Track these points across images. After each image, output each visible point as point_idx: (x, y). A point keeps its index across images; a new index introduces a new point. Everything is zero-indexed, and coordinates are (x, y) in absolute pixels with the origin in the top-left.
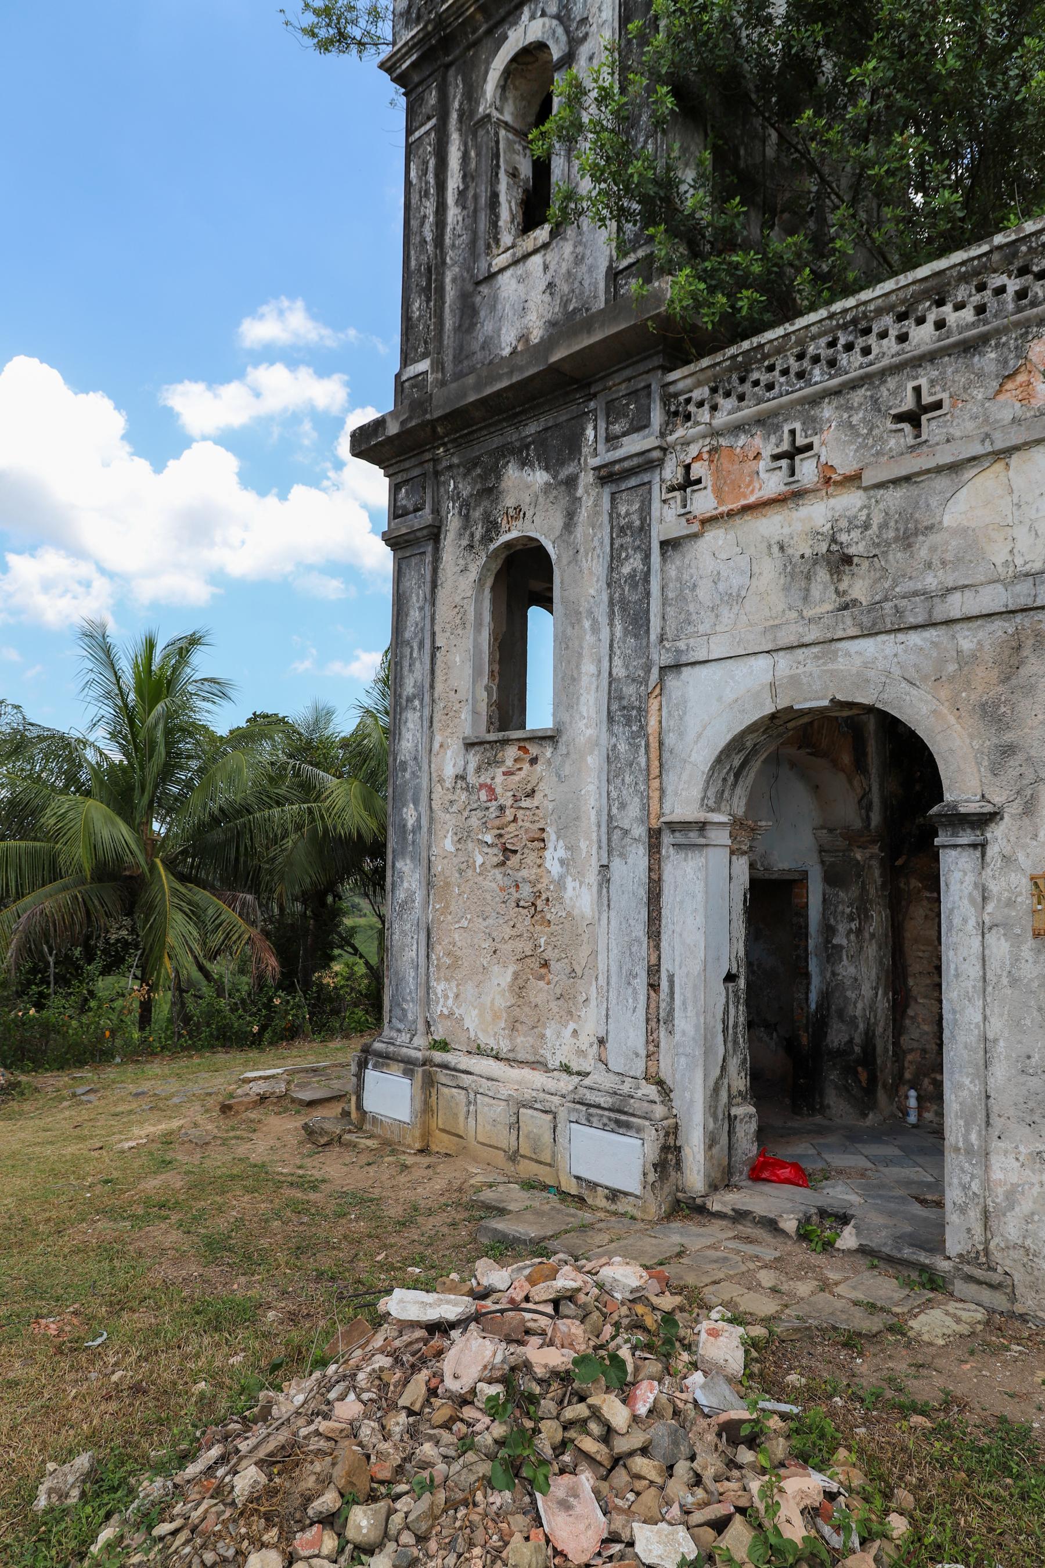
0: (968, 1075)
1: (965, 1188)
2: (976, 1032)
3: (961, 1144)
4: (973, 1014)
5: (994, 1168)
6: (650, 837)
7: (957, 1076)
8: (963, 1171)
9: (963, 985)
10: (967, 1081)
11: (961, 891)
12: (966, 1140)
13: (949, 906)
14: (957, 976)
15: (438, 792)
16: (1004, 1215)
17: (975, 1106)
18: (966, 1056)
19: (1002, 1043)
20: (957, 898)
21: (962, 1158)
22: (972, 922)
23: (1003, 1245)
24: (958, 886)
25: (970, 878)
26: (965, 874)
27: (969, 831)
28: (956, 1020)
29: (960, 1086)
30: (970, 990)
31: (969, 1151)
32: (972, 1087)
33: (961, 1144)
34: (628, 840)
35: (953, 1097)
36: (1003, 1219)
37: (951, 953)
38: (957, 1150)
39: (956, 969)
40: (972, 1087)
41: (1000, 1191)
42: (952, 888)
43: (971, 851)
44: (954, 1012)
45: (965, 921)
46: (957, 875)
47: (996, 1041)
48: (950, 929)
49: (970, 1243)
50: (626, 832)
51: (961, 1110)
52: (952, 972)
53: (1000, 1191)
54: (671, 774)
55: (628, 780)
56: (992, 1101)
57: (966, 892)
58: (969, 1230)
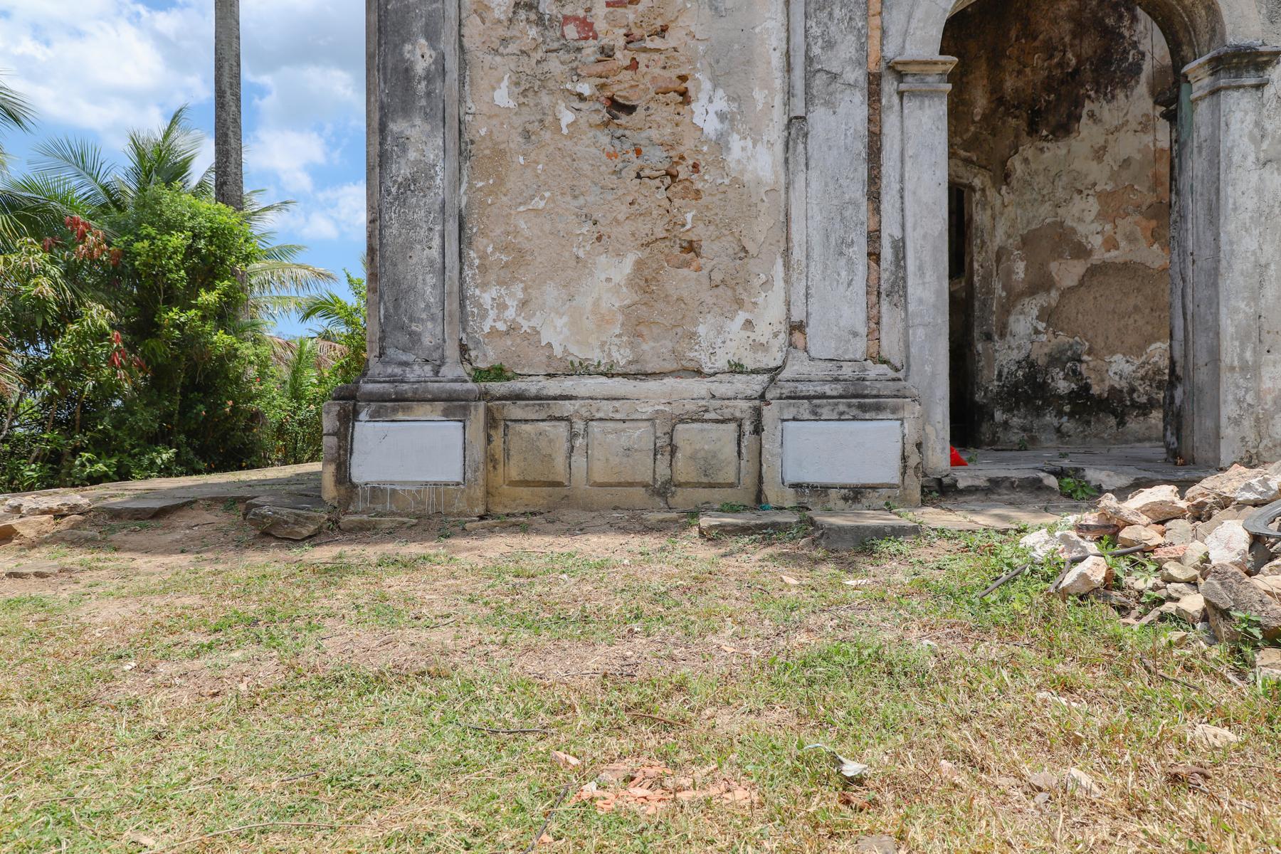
0: (1243, 300)
1: (1239, 402)
2: (1253, 259)
3: (1236, 363)
4: (1249, 243)
5: (1264, 379)
6: (870, 83)
7: (1233, 302)
8: (1238, 387)
9: (1241, 217)
10: (1242, 305)
11: (1242, 129)
12: (1241, 358)
13: (1229, 144)
14: (1235, 209)
15: (473, 28)
16: (1272, 418)
17: (1249, 326)
18: (1241, 282)
19: (1273, 267)
20: (1237, 137)
21: (1236, 375)
22: (1251, 158)
23: (1270, 445)
24: (1238, 125)
25: (1251, 118)
26: (1246, 113)
27: (1253, 72)
28: (1232, 251)
29: (1236, 310)
30: (1248, 221)
31: (1244, 368)
32: (1247, 309)
33: (1236, 363)
34: (837, 86)
35: (1229, 322)
36: (1271, 422)
37: (1230, 189)
38: (1232, 369)
39: (1235, 203)
40: (1247, 309)
41: (1269, 398)
42: (1232, 127)
43: (1253, 91)
44: (1231, 243)
45: (1245, 157)
46: (1239, 115)
47: (1267, 265)
48: (1229, 166)
49: (1244, 449)
50: (834, 77)
51: (1237, 332)
52: (1230, 206)
53: (1269, 398)
54: (894, 12)
55: (837, 13)
56: (1262, 319)
57: (1247, 131)
58: (1243, 439)
